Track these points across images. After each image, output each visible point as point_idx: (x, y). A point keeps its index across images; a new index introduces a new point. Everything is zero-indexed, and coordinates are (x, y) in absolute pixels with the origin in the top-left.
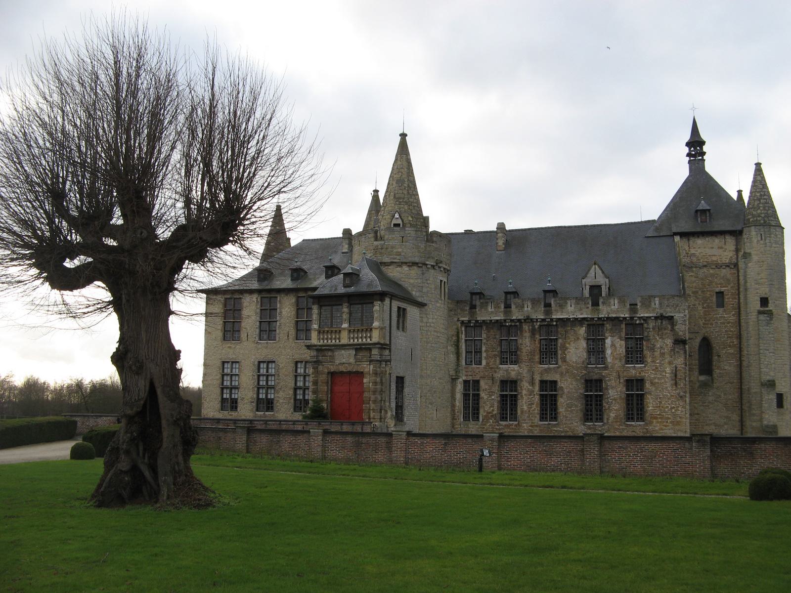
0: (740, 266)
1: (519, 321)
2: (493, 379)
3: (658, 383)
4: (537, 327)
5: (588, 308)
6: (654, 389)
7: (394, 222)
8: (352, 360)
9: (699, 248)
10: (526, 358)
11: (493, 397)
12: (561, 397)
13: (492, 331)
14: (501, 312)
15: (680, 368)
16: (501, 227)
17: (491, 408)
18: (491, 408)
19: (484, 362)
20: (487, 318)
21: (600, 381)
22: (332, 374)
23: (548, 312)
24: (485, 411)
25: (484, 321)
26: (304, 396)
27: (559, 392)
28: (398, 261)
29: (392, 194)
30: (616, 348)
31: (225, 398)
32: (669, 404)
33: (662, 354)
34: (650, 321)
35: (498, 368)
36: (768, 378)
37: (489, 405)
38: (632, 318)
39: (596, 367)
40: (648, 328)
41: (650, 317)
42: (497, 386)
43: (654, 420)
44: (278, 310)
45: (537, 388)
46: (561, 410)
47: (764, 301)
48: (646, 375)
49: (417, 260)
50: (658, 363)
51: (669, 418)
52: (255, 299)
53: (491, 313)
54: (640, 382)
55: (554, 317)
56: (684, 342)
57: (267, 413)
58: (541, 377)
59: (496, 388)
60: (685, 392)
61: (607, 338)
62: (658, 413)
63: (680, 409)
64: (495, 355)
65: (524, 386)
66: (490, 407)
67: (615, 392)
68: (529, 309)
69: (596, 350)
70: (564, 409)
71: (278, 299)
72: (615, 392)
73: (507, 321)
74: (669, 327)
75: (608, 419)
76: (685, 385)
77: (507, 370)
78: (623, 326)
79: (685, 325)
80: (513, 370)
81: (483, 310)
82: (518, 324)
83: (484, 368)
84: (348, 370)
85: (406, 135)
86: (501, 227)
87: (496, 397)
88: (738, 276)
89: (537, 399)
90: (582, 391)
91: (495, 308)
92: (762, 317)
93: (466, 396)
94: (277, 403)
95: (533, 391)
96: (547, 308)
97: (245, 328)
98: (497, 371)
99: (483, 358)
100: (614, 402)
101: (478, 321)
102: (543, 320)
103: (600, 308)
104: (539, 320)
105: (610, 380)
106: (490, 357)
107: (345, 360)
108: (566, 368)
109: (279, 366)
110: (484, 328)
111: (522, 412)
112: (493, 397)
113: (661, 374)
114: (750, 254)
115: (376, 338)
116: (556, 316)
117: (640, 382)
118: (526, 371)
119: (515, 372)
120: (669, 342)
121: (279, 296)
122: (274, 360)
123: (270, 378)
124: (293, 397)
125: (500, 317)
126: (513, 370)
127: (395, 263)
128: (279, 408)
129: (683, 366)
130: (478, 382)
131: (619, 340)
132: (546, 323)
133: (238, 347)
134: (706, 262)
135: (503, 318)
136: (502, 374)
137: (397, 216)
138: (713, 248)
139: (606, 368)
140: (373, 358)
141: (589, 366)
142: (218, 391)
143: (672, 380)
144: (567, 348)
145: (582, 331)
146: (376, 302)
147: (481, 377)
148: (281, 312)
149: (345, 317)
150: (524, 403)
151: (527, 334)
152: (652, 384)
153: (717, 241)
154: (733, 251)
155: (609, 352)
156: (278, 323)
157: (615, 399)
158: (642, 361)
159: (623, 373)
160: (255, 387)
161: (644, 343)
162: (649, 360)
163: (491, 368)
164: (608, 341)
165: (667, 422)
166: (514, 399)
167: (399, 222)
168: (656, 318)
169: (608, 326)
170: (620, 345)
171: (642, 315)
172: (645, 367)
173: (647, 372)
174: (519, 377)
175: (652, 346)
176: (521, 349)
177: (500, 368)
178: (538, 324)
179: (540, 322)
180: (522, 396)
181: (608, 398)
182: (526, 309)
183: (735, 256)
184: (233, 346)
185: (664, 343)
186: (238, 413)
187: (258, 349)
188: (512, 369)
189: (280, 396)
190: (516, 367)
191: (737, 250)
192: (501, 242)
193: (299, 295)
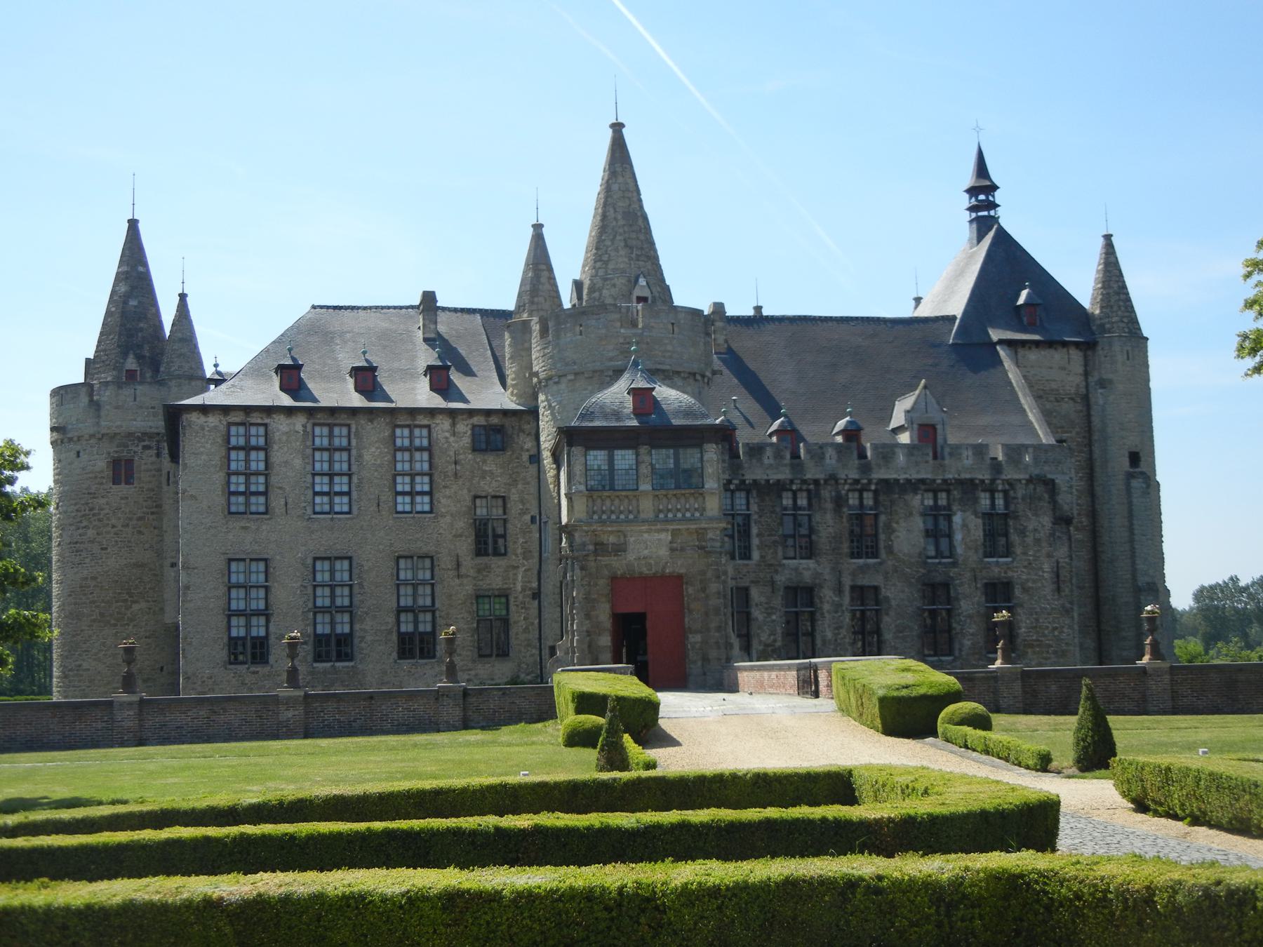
0: (1092, 400)
1: (816, 482)
2: (773, 583)
3: (1032, 588)
4: (843, 492)
5: (927, 462)
6: (1026, 598)
7: (637, 292)
8: (664, 552)
9: (1032, 367)
10: (828, 548)
11: (774, 617)
12: (887, 614)
13: (767, 499)
14: (785, 465)
15: (1064, 564)
16: (719, 308)
17: (772, 637)
18: (772, 637)
19: (756, 555)
21: (946, 586)
22: (614, 579)
24: (760, 642)
25: (755, 481)
26: (416, 626)
28: (668, 367)
29: (618, 238)
30: (969, 531)
31: (235, 638)
32: (1050, 623)
34: (1018, 486)
35: (781, 565)
36: (1147, 579)
37: (768, 632)
38: (993, 481)
39: (940, 563)
40: (1015, 498)
41: (1020, 480)
42: (780, 598)
43: (1030, 650)
44: (354, 452)
45: (847, 600)
47: (1135, 458)
48: (1015, 574)
49: (695, 367)
50: (1031, 555)
51: (1050, 646)
52: (299, 428)
56: (1068, 521)
57: (338, 664)
58: (853, 580)
59: (778, 601)
60: (1071, 603)
61: (955, 514)
62: (1034, 638)
63: (1065, 630)
64: (775, 542)
65: (825, 596)
66: (770, 635)
68: (834, 462)
70: (891, 635)
71: (353, 430)
73: (796, 481)
74: (1046, 496)
75: (960, 650)
76: (1072, 591)
77: (796, 569)
79: (1071, 493)
80: (808, 568)
81: (754, 461)
82: (812, 487)
83: (756, 565)
84: (654, 571)
85: (621, 125)
86: (719, 308)
88: (1089, 416)
89: (848, 616)
90: (918, 603)
91: (775, 458)
92: (1136, 483)
94: (361, 642)
95: (841, 605)
96: (863, 461)
97: (280, 488)
98: (780, 569)
99: (754, 547)
100: (968, 621)
101: (744, 481)
102: (857, 482)
103: (946, 462)
104: (849, 481)
105: (962, 584)
106: (766, 546)
108: (894, 565)
109: (362, 566)
110: (754, 493)
112: (774, 617)
113: (1036, 574)
114: (1111, 382)
115: (712, 510)
116: (880, 474)
118: (828, 570)
119: (810, 572)
120: (1047, 520)
121: (353, 422)
122: (349, 554)
123: (338, 591)
124: (395, 628)
125: (784, 474)
126: (808, 568)
127: (663, 371)
128: (365, 652)
129: (1067, 560)
131: (973, 517)
132: (859, 487)
133: (264, 527)
134: (1043, 390)
135: (790, 476)
136: (788, 576)
137: (642, 282)
138: (1051, 368)
139: (955, 564)
141: (929, 561)
143: (1054, 583)
144: (894, 531)
146: (710, 445)
147: (752, 582)
148: (360, 456)
149: (645, 471)
150: (826, 626)
151: (829, 506)
152: (1025, 590)
153: (1058, 356)
154: (1081, 375)
155: (958, 537)
156: (355, 479)
157: (970, 617)
158: (1008, 552)
159: (981, 572)
160: (309, 611)
161: (1011, 523)
162: (1018, 550)
163: (771, 565)
164: (957, 519)
165: (1048, 652)
167: (646, 293)
169: (955, 492)
170: (975, 526)
171: (1009, 477)
172: (1012, 562)
173: (1015, 569)
174: (817, 581)
175: (1022, 527)
177: (784, 565)
178: (847, 487)
179: (850, 484)
180: (823, 614)
181: (959, 615)
182: (828, 461)
183: (1084, 383)
184: (253, 526)
185: (1040, 522)
186: (272, 667)
187: (312, 532)
188: (805, 566)
189: (367, 628)
190: (811, 563)
191: (1086, 374)
193: (399, 423)
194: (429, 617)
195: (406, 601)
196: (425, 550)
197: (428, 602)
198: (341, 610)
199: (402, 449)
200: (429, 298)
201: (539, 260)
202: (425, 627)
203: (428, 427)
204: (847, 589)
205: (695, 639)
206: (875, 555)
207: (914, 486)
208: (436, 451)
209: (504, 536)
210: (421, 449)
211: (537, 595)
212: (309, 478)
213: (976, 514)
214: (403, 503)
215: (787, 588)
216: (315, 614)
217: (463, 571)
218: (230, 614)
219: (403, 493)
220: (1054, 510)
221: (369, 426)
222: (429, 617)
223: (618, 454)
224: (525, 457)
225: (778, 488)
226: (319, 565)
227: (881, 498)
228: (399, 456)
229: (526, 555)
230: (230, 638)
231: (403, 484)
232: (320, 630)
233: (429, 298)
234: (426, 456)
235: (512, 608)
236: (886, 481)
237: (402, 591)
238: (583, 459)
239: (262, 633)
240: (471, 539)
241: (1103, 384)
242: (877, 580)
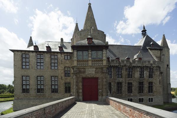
0: (161, 57)
1: (123, 66)
8: (94, 73)
19: (112, 77)
20: (113, 65)
21: (143, 83)
22: (84, 79)
27: (133, 86)
33: (157, 76)
35: (117, 79)
38: (151, 66)
45: (127, 85)
54: (152, 83)
56: (162, 73)
59: (116, 85)
67: (146, 86)
69: (142, 75)
71: (44, 55)
72: (146, 86)
78: (148, 69)
80: (121, 80)
89: (127, 87)
102: (129, 66)
103: (144, 63)
107: (91, 72)
117: (152, 83)
120: (159, 73)
123: (41, 82)
125: (117, 65)
130: (111, 83)
140: (104, 71)
142: (21, 86)
145: (138, 69)
152: (155, 83)
155: (145, 75)
156: (44, 63)
161: (153, 73)
162: (154, 77)
164: (145, 72)
168: (156, 67)
176: (122, 74)
184: (26, 71)
190: (121, 79)
191: (160, 54)
194: (57, 86)
196: (56, 75)
197: (57, 84)
198: (42, 85)
203: (57, 55)
204: (127, 83)
207: (138, 67)
208: (58, 59)
210: (56, 59)
212: (36, 63)
213: (148, 71)
214: (53, 68)
215: (117, 83)
216: (37, 85)
217: (63, 79)
218: (23, 85)
219: (53, 66)
220: (160, 71)
221: (47, 55)
222: (57, 86)
226: (38, 77)
227: (133, 69)
228: (52, 60)
230: (23, 88)
231: (53, 65)
232: (38, 88)
234: (57, 60)
235: (71, 85)
236: (134, 66)
237: (52, 82)
238: (76, 53)
239: (28, 88)
241: (163, 55)
242: (132, 82)
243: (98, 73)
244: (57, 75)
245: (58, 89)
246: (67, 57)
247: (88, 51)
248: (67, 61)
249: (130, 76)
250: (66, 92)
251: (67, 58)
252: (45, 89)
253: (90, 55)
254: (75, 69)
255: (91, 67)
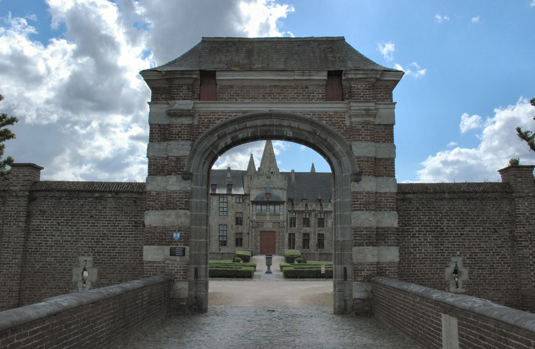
2: (300, 232)
7: (271, 171)
8: (271, 227)
19: (297, 226)
20: (298, 209)
22: (261, 231)
23: (322, 208)
27: (325, 238)
46: (325, 244)
49: (282, 187)
53: (300, 207)
55: (324, 210)
59: (301, 236)
80: (307, 230)
86: (293, 171)
87: (301, 240)
89: (317, 240)
93: (290, 239)
107: (268, 226)
111: (311, 245)
125: (304, 209)
126: (307, 230)
130: (294, 234)
137: (272, 168)
140: (280, 226)
148: (212, 203)
166: (308, 240)
167: (273, 171)
190: (309, 228)
192: (293, 178)
194: (226, 237)
195: (221, 234)
196: (225, 223)
199: (221, 202)
200: (229, 168)
201: (252, 162)
202: (225, 240)
205: (277, 244)
206: (324, 227)
208: (228, 203)
209: (242, 221)
210: (225, 202)
211: (248, 234)
215: (303, 234)
222: (226, 237)
223: (263, 206)
224: (247, 204)
225: (303, 212)
227: (325, 214)
229: (247, 225)
231: (221, 210)
233: (229, 168)
234: (226, 204)
235: (243, 236)
236: (326, 211)
240: (235, 221)
242: (324, 233)
243: (275, 227)
244: (226, 223)
245: (226, 241)
246: (239, 199)
247: (266, 205)
248: (240, 204)
249: (321, 223)
250: (237, 245)
251: (239, 201)
252: (212, 242)
253: (268, 210)
254: (254, 223)
255: (270, 221)
